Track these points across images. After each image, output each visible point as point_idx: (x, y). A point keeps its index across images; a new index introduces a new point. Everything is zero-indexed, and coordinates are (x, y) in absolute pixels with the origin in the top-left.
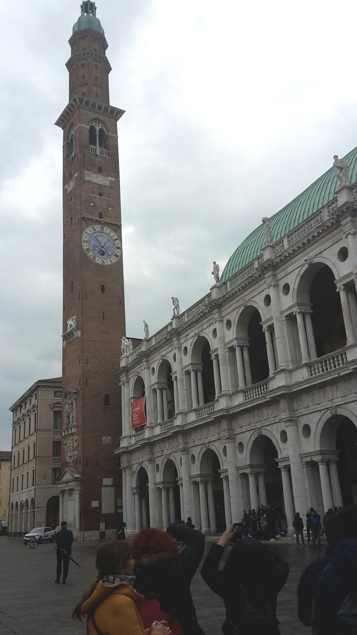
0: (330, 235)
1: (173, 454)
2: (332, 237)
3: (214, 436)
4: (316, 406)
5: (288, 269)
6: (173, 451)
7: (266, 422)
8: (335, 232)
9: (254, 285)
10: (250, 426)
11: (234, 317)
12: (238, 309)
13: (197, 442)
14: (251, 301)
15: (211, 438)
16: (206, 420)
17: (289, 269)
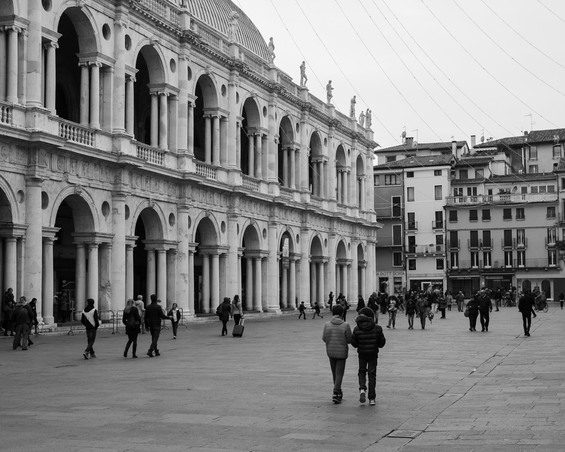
0: (264, 91)
1: (87, 189)
2: (264, 93)
3: (163, 195)
4: (245, 213)
5: (242, 83)
6: (92, 185)
7: (214, 207)
8: (266, 92)
9: (219, 63)
10: (201, 204)
11: (198, 73)
12: (200, 68)
13: (138, 192)
14: (212, 74)
15: (160, 196)
16: (172, 174)
17: (243, 84)
